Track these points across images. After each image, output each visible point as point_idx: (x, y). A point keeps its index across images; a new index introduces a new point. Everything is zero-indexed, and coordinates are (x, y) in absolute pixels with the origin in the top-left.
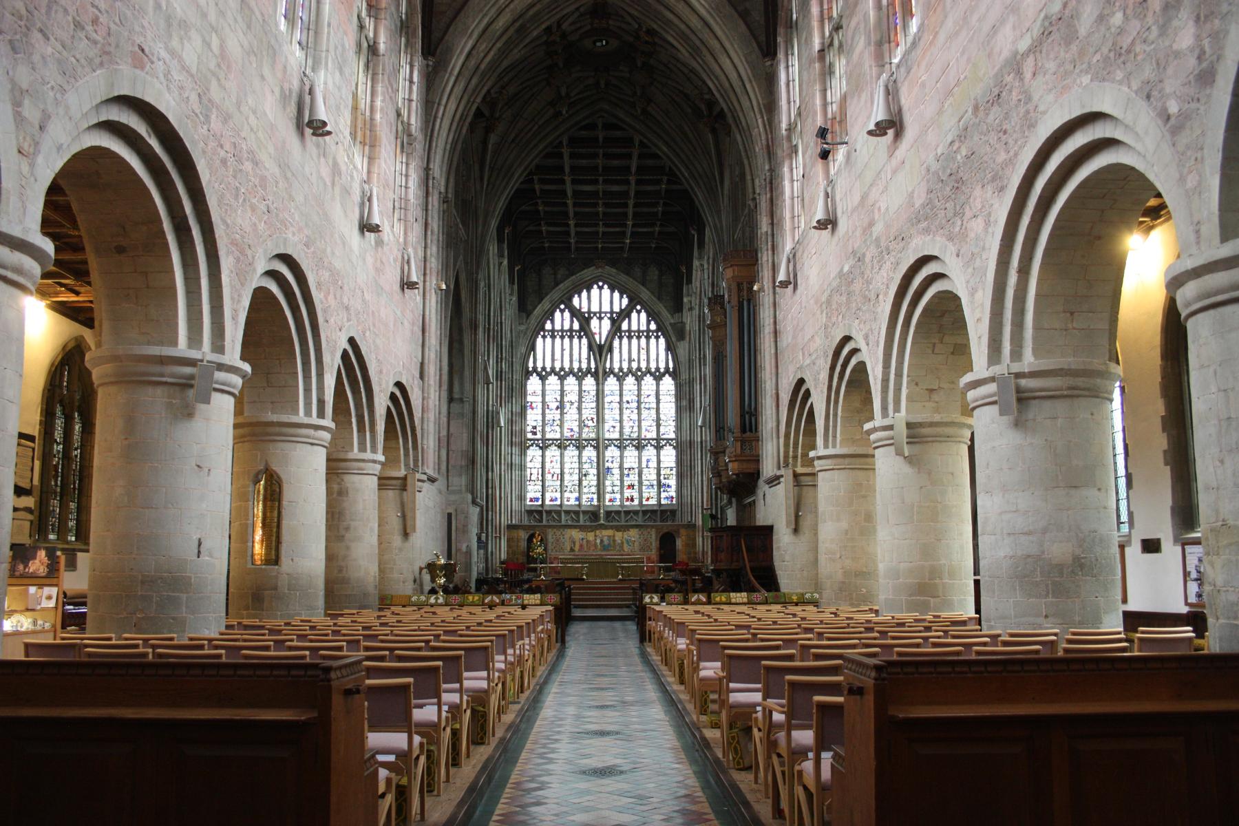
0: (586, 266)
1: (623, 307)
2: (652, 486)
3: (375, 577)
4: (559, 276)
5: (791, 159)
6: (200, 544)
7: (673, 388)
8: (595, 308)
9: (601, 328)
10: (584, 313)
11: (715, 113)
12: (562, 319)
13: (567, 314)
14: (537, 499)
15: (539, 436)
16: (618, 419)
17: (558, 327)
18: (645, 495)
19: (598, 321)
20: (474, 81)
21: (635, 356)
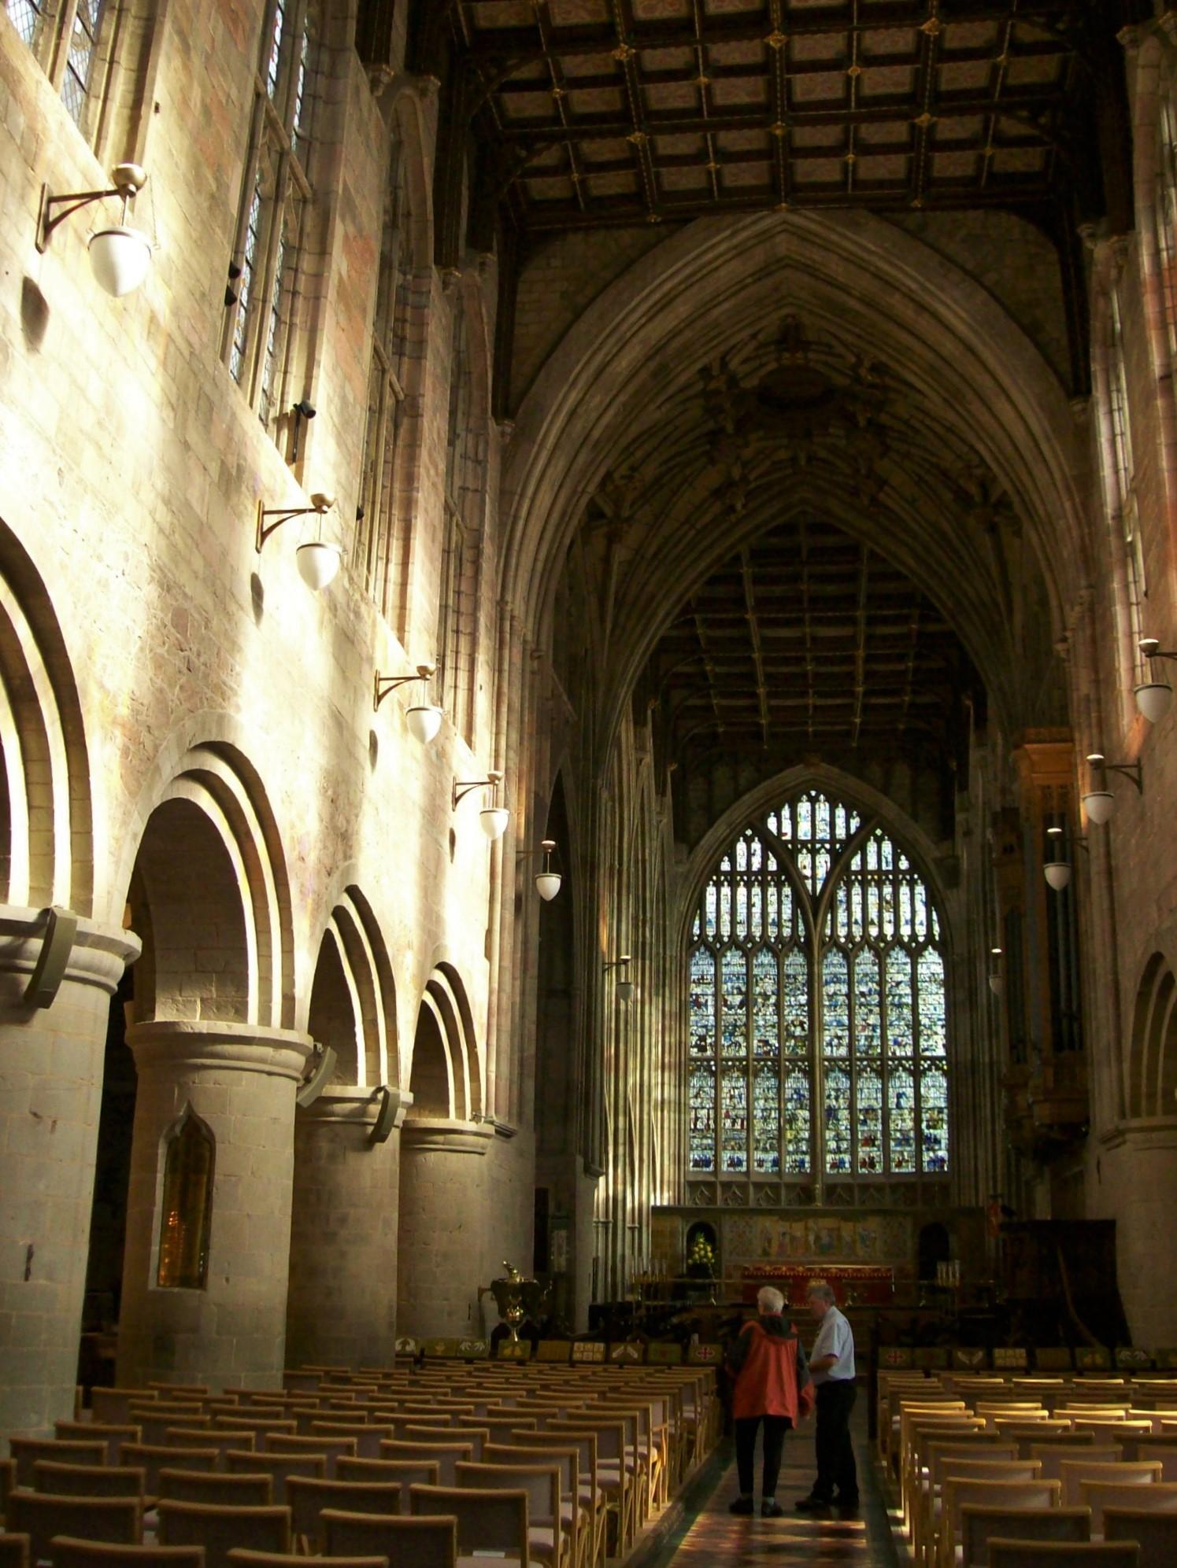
0: (789, 763)
1: (853, 830)
3: (391, 1307)
5: (1125, 566)
6: (30, 1255)
7: (939, 970)
9: (816, 867)
10: (787, 842)
11: (993, 499)
12: (747, 854)
13: (756, 846)
14: (707, 1163)
17: (741, 865)
18: (895, 1157)
20: (582, 459)
21: (873, 913)
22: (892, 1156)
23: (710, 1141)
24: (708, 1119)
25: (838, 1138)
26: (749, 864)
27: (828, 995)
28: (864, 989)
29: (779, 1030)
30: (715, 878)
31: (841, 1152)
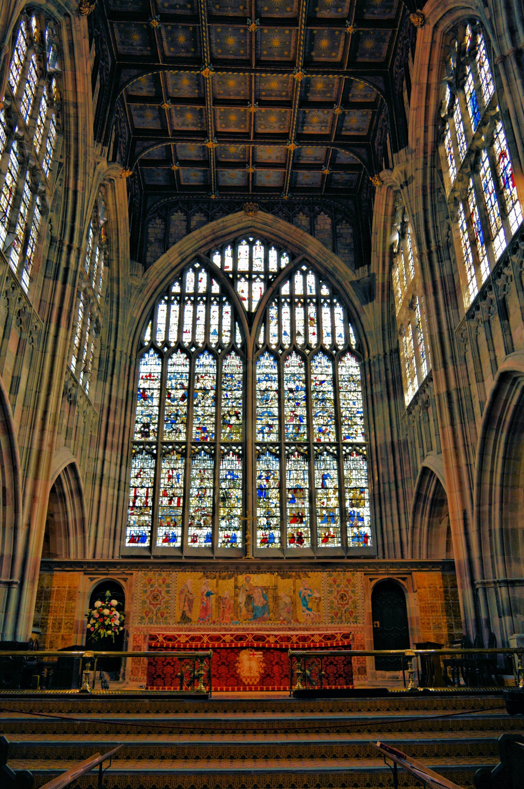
1: (283, 266)
2: (333, 517)
4: (193, 223)
7: (356, 372)
8: (243, 266)
10: (227, 273)
13: (203, 275)
14: (142, 538)
15: (152, 438)
16: (277, 414)
17: (190, 288)
19: (247, 283)
21: (300, 327)
22: (319, 531)
23: (147, 518)
24: (147, 497)
25: (269, 516)
26: (196, 287)
27: (260, 391)
28: (292, 386)
29: (216, 418)
30: (166, 298)
31: (271, 528)
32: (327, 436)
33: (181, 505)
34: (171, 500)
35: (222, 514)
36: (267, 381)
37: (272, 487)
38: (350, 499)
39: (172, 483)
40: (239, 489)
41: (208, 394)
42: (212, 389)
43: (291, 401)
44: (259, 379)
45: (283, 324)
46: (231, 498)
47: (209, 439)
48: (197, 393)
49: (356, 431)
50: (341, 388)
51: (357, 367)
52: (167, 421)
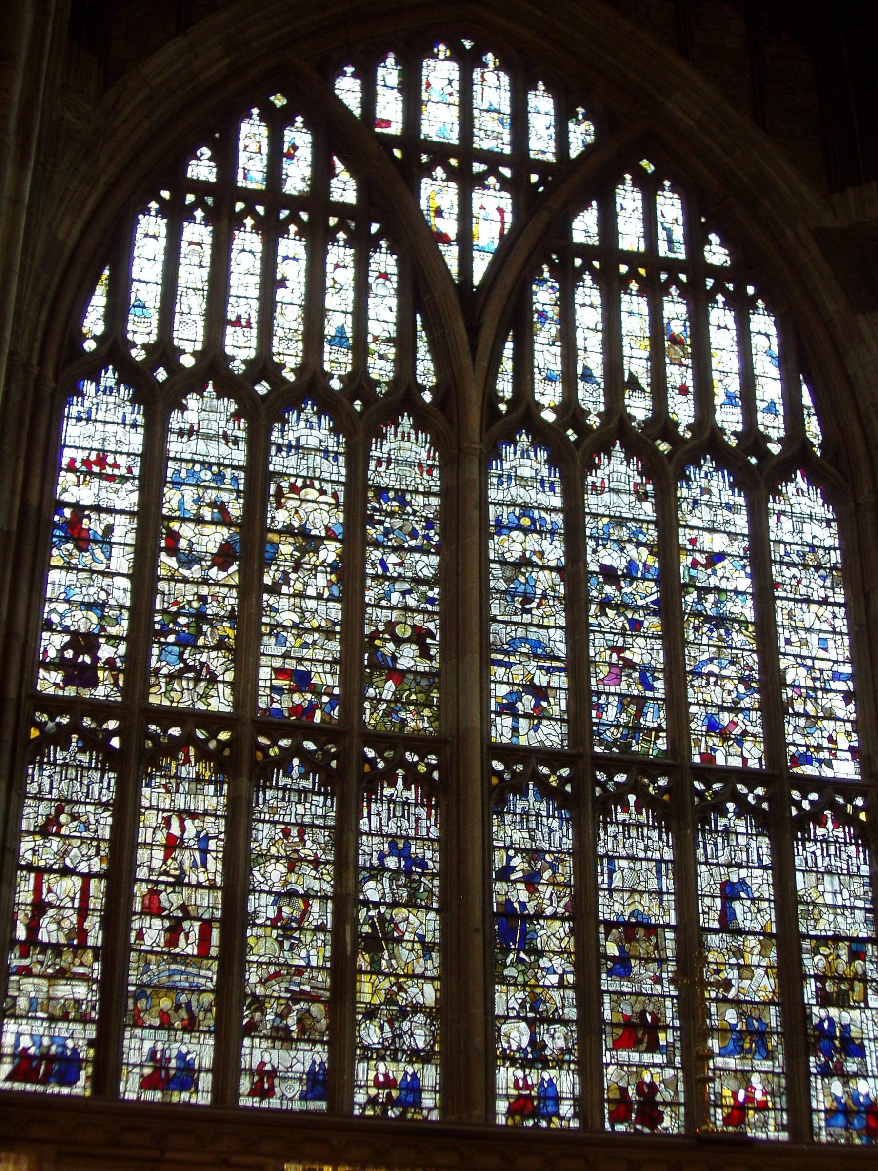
1: (575, 150)
2: (761, 1035)
7: (827, 536)
10: (390, 141)
16: (561, 649)
23: (81, 990)
24: (83, 912)
26: (275, 174)
27: (503, 563)
28: (611, 557)
31: (545, 1064)
32: (735, 749)
33: (214, 951)
34: (174, 932)
35: (367, 998)
36: (526, 531)
37: (549, 911)
38: (817, 977)
39: (181, 867)
40: (428, 908)
41: (316, 552)
42: (331, 535)
43: (611, 613)
44: (498, 521)
45: (580, 343)
46: (400, 940)
47: (318, 717)
48: (276, 546)
49: (831, 739)
50: (777, 585)
51: (828, 522)
52: (165, 632)
